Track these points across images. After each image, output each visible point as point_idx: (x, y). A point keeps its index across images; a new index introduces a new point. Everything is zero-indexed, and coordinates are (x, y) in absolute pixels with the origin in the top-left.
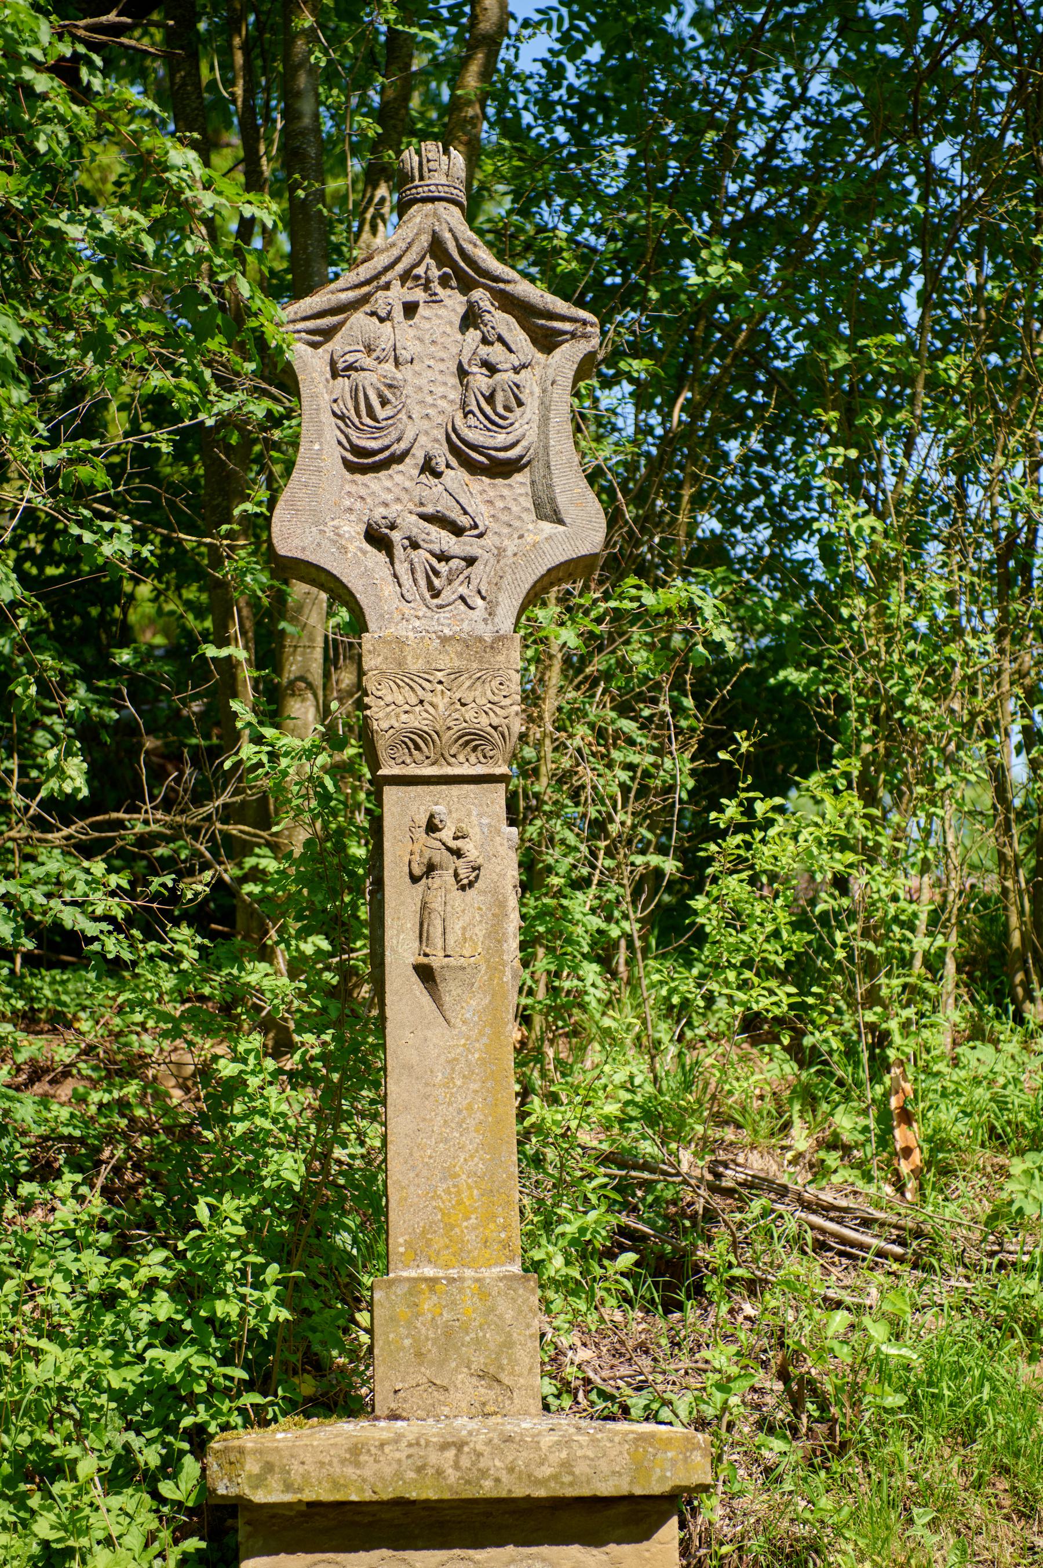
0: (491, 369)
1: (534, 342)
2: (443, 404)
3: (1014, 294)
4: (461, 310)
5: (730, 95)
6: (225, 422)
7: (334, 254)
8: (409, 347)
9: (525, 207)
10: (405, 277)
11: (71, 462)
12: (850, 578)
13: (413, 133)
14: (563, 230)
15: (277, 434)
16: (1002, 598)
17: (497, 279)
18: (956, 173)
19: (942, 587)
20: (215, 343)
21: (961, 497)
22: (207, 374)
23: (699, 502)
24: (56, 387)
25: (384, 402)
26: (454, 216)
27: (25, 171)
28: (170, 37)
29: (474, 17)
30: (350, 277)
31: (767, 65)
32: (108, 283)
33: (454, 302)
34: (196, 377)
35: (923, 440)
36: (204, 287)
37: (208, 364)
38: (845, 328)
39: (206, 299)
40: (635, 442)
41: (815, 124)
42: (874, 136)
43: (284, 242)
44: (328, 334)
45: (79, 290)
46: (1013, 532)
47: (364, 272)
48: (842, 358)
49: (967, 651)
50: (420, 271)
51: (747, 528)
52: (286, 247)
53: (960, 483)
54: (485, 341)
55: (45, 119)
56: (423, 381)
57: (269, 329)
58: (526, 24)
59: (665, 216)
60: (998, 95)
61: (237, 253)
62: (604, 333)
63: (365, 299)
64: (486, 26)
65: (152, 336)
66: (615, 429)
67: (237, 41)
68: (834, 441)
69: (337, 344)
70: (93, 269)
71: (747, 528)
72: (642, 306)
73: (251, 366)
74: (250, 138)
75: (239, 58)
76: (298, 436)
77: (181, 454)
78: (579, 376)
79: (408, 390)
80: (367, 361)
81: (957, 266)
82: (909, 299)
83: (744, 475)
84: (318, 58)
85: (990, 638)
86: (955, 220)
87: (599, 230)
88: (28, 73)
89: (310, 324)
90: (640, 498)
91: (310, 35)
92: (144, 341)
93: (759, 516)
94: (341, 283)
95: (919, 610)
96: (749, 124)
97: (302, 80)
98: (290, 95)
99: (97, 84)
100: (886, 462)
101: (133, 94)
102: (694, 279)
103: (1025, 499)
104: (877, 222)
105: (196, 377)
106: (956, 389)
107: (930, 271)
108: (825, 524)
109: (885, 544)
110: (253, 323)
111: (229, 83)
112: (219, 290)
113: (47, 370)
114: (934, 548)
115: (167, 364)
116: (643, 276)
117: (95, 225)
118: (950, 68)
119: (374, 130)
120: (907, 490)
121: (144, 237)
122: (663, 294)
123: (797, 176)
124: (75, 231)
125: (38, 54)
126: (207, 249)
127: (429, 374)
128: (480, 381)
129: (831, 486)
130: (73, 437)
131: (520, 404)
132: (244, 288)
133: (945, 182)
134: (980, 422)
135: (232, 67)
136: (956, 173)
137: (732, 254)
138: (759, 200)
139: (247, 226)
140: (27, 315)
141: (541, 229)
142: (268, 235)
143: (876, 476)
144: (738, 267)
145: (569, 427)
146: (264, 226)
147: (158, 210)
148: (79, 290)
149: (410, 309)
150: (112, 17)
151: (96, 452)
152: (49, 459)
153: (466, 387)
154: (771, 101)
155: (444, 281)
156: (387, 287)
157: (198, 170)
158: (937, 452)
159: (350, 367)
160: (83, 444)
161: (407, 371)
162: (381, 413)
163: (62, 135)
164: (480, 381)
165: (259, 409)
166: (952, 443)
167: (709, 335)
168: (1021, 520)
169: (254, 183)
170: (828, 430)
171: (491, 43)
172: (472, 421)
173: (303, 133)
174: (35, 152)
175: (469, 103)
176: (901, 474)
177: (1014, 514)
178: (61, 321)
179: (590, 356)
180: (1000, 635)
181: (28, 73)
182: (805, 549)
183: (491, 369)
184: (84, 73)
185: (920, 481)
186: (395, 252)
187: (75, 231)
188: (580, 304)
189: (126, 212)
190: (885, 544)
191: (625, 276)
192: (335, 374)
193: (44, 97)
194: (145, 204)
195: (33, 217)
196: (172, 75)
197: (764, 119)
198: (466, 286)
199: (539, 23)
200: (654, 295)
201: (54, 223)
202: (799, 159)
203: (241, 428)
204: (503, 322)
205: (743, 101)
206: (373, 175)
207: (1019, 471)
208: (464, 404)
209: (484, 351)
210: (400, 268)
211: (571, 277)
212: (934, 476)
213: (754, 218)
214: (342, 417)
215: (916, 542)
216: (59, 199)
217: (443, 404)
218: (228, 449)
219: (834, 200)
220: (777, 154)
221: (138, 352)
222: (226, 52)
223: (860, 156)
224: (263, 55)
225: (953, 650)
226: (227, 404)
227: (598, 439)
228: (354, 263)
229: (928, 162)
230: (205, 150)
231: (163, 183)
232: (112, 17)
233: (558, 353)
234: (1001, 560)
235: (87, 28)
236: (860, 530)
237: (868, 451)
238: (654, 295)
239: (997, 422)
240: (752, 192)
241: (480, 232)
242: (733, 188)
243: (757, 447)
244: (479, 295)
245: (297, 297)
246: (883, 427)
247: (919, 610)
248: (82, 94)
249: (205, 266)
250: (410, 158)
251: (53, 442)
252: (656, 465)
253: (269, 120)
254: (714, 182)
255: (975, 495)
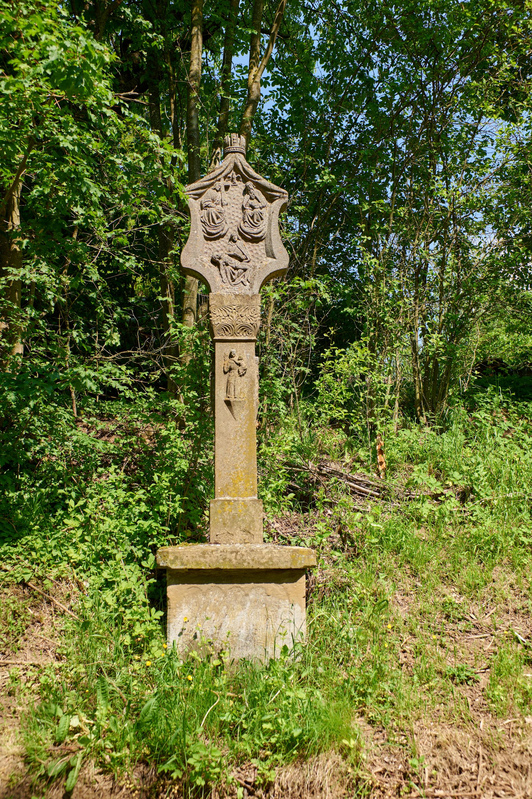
0: (253, 208)
1: (267, 199)
2: (237, 219)
3: (422, 189)
4: (243, 188)
5: (331, 121)
6: (166, 224)
7: (203, 171)
8: (226, 200)
9: (265, 154)
10: (225, 177)
11: (116, 236)
12: (368, 279)
13: (229, 131)
14: (277, 164)
15: (183, 228)
16: (416, 286)
17: (255, 178)
18: (404, 149)
19: (397, 282)
20: (163, 199)
21: (404, 253)
22: (160, 208)
23: (319, 253)
24: (112, 212)
25: (218, 218)
26: (241, 158)
27: (103, 142)
28: (151, 99)
29: (249, 95)
30: (208, 177)
31: (344, 112)
32: (129, 178)
33: (241, 186)
34: (156, 209)
35: (392, 235)
36: (160, 180)
37: (161, 205)
38: (367, 198)
39: (161, 184)
40: (299, 233)
41: (359, 132)
42: (378, 138)
43: (186, 168)
44: (200, 195)
45: (120, 180)
46: (420, 265)
47: (212, 175)
48: (366, 207)
49: (405, 303)
50: (230, 175)
51: (335, 262)
52: (187, 169)
53: (404, 248)
54: (251, 199)
55: (110, 125)
56: (230, 211)
57: (181, 194)
58: (266, 97)
59: (310, 159)
60: (417, 124)
61: (171, 168)
62: (289, 197)
63: (212, 184)
64: (253, 97)
65: (142, 196)
66: (293, 229)
67: (172, 101)
68: (363, 234)
69: (203, 199)
70: (124, 173)
71: (335, 262)
72: (301, 189)
73: (175, 206)
74: (176, 132)
75: (173, 106)
76: (189, 229)
77: (151, 235)
78: (281, 210)
79: (226, 214)
80: (213, 204)
81: (404, 179)
82: (388, 189)
83: (334, 245)
84: (198, 106)
85: (412, 299)
86: (404, 164)
87: (289, 164)
88: (104, 110)
89: (194, 192)
90: (300, 252)
91: (196, 99)
92: (140, 197)
93: (339, 259)
94: (204, 179)
95: (390, 289)
96: (338, 131)
97: (193, 113)
98: (189, 119)
99: (127, 113)
100: (380, 242)
101: (138, 118)
102: (319, 180)
103: (424, 254)
104: (378, 164)
105: (156, 209)
106: (403, 218)
107: (395, 180)
108: (360, 261)
109: (380, 268)
110: (175, 192)
111: (169, 114)
112: (165, 180)
113: (109, 207)
114: (395, 270)
115: (147, 205)
116: (304, 180)
117: (125, 159)
118: (402, 116)
119: (216, 130)
120: (387, 251)
121: (141, 163)
122: (309, 185)
123: (353, 148)
124: (118, 161)
125: (108, 104)
126: (161, 167)
127: (233, 209)
128: (249, 211)
129: (362, 249)
130: (117, 228)
131: (262, 219)
132: (173, 180)
133: (400, 152)
134: (410, 229)
135: (170, 109)
136: (404, 149)
137: (331, 173)
138: (341, 156)
139: (174, 160)
140: (103, 187)
141: (270, 163)
142: (181, 164)
143: (377, 246)
144: (333, 177)
145: (278, 228)
146: (180, 161)
147: (146, 154)
148: (120, 180)
149: (227, 188)
150: (132, 92)
151: (125, 233)
152: (109, 235)
153: (245, 213)
154: (345, 124)
155: (238, 179)
156: (219, 180)
157: (159, 141)
158: (396, 239)
159: (207, 206)
160: (120, 230)
161: (225, 208)
162: (217, 221)
163: (115, 131)
164: (249, 211)
165: (177, 220)
166: (402, 235)
167: (324, 199)
168: (423, 261)
169: (177, 146)
170: (361, 231)
171: (254, 103)
172: (246, 224)
173: (193, 131)
174: (107, 136)
175: (247, 122)
176: (384, 245)
177: (421, 259)
178: (113, 191)
179: (285, 204)
180: (415, 298)
181: (104, 110)
182: (353, 269)
183: (253, 208)
184: (123, 109)
185: (391, 248)
186: (222, 169)
187: (118, 161)
188: (282, 187)
189: (135, 154)
190: (380, 268)
191: (297, 180)
192: (202, 209)
193: (110, 117)
194: (141, 153)
195: (105, 156)
196: (151, 112)
197: (343, 130)
198: (245, 180)
199: (270, 96)
200: (306, 185)
201: (111, 158)
202: (354, 143)
203: (171, 226)
204: (257, 192)
205: (336, 124)
206: (215, 145)
207: (422, 245)
208: (244, 219)
209: (250, 202)
210: (224, 174)
211: (279, 179)
212: (396, 246)
213: (339, 162)
214: (204, 223)
215: (389, 268)
216: (112, 152)
217: (237, 219)
218: (167, 233)
219: (365, 156)
220: (347, 141)
221: (138, 201)
222: (169, 104)
223: (373, 142)
224: (181, 105)
225: (400, 303)
226: (166, 218)
227: (287, 232)
228: (208, 173)
229: (395, 144)
230: (162, 136)
231: (146, 145)
232: (132, 92)
233: (274, 203)
234: (416, 274)
235: (124, 96)
236: (371, 263)
237: (374, 238)
238: (306, 185)
239: (416, 229)
240: (338, 153)
241: (250, 164)
242: (332, 152)
243: (339, 236)
244: (249, 183)
245: (190, 183)
246: (379, 230)
247: (390, 289)
248: (121, 116)
249: (160, 173)
250: (227, 138)
251: (110, 229)
252: (306, 241)
253: (182, 125)
254: (326, 150)
255: (408, 253)
